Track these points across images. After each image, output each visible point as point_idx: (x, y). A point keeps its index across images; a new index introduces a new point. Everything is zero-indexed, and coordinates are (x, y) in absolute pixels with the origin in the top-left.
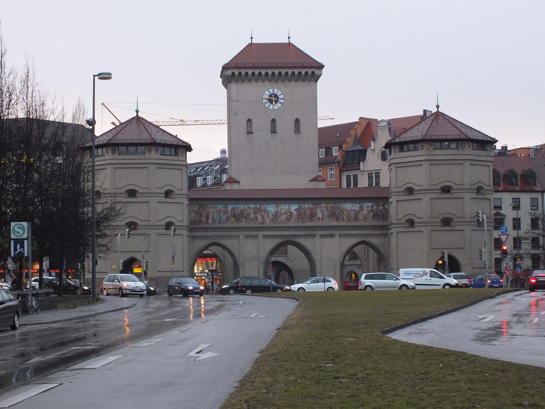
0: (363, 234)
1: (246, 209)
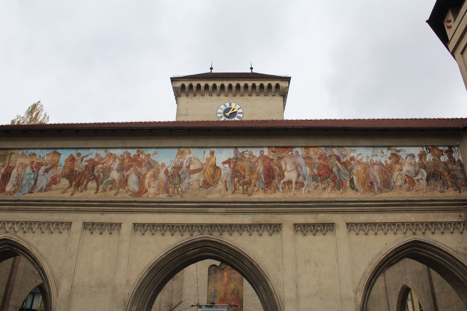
0: (412, 223)
1: (102, 159)
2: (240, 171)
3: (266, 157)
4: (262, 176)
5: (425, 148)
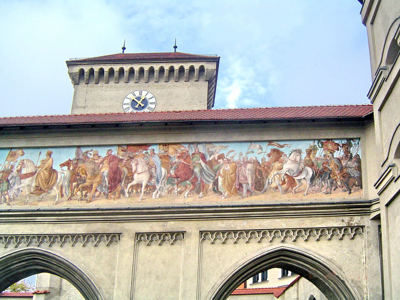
2: (81, 174)
3: (114, 157)
4: (106, 179)
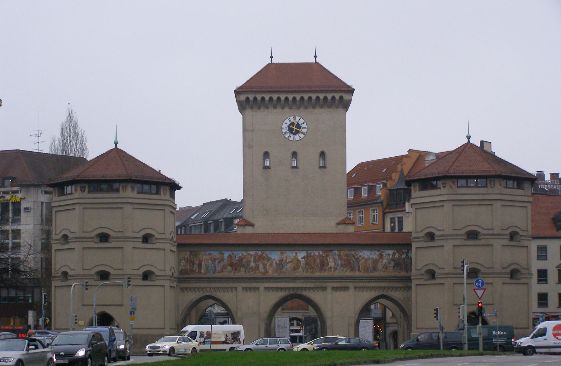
0: (383, 287)
3: (321, 255)
4: (319, 265)
5: (396, 251)
